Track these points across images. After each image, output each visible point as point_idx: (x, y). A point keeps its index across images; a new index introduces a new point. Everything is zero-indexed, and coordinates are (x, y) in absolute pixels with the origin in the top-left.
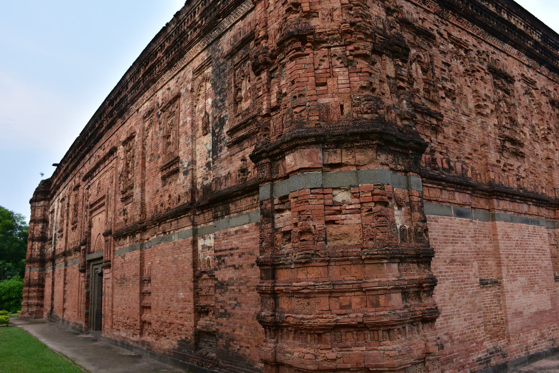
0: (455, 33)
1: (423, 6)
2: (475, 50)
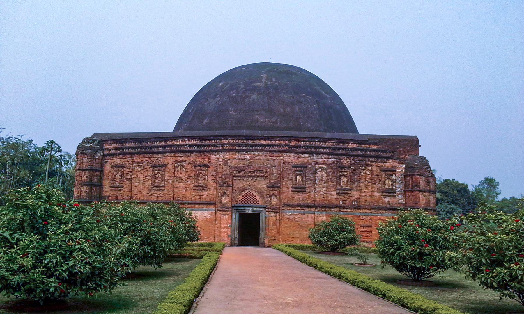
0: (136, 161)
1: (123, 158)
2: (146, 162)
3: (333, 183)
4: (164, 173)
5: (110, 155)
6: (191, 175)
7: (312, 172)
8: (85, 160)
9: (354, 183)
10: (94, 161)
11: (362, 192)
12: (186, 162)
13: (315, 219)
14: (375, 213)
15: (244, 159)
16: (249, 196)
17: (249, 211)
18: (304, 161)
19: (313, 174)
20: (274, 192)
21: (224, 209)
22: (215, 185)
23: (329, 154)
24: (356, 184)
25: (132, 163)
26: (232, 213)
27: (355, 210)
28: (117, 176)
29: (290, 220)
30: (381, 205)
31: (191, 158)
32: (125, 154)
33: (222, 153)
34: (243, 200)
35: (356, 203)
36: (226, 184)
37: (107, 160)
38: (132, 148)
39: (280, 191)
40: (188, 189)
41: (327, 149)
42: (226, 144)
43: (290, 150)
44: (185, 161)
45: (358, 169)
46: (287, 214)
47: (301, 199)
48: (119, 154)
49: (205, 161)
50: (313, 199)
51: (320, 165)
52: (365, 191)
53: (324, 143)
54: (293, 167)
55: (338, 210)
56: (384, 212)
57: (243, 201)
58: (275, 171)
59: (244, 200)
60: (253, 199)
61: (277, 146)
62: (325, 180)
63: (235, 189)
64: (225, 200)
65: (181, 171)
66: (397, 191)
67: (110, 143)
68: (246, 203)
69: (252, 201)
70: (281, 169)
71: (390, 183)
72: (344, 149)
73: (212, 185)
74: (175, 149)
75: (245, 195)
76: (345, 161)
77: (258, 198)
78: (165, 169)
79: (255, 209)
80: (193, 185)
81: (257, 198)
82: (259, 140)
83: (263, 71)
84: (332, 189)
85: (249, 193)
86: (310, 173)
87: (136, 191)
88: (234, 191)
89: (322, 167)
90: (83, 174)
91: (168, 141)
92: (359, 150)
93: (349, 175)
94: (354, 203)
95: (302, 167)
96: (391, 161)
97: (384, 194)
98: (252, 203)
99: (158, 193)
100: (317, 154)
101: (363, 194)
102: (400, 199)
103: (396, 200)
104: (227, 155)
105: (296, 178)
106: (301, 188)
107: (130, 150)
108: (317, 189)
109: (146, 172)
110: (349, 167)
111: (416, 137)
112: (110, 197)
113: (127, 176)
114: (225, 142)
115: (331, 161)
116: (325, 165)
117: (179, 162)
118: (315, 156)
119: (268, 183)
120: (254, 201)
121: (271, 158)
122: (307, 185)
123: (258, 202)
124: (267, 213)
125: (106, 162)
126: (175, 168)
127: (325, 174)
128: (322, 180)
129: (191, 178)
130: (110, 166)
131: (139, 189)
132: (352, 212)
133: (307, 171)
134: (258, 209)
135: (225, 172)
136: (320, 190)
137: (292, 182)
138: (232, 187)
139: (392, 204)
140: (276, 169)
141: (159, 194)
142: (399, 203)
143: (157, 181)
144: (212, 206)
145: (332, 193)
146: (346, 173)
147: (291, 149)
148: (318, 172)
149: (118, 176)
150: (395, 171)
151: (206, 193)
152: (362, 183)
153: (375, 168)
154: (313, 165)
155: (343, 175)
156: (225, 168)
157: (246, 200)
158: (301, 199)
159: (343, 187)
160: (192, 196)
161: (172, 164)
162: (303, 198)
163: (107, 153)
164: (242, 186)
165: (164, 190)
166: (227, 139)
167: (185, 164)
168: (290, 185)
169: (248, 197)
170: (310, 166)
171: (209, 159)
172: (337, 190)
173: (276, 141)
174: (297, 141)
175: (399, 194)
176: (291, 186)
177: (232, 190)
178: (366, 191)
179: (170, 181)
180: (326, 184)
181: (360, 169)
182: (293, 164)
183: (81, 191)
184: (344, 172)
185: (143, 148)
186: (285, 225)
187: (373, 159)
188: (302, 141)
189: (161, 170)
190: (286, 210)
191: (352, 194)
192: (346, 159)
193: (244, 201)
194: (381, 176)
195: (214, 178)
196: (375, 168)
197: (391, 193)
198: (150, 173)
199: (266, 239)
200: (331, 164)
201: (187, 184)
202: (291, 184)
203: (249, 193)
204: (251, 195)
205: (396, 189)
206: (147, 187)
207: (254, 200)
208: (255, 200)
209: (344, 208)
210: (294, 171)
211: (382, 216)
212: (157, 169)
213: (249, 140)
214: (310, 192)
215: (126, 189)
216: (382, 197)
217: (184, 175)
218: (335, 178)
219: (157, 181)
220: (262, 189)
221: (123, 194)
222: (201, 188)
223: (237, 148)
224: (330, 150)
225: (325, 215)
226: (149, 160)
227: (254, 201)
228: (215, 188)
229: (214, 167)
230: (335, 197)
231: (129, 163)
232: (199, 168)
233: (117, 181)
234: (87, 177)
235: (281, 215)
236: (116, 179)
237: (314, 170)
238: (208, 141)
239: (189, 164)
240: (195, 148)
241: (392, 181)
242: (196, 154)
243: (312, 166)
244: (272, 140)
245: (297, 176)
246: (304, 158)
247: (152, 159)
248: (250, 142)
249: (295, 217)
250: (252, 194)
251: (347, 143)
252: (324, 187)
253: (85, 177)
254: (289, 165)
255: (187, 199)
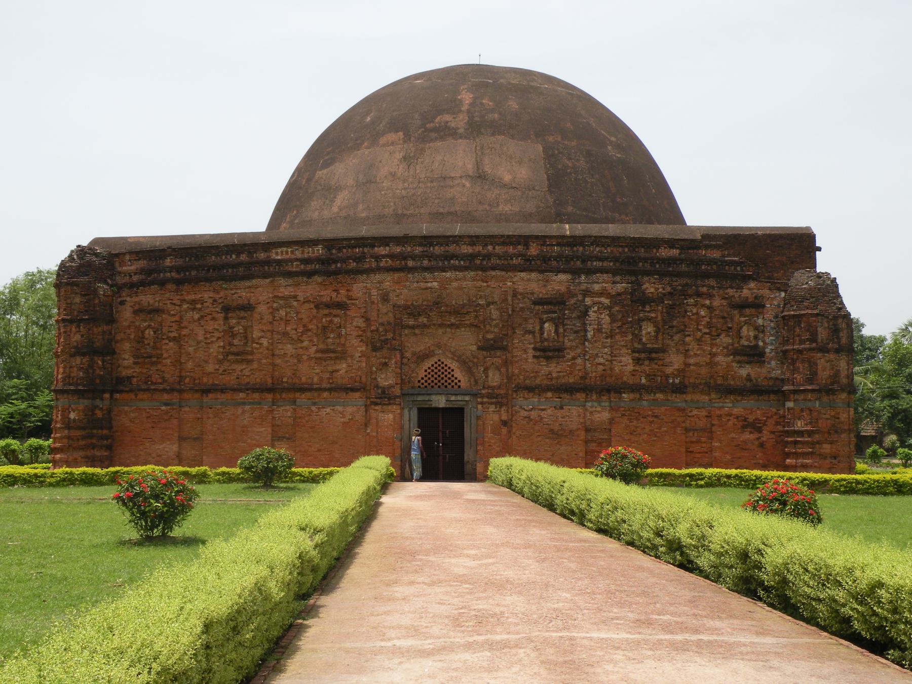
0: (191, 297)
2: (211, 301)
3: (625, 338)
4: (249, 324)
5: (131, 286)
6: (310, 327)
7: (579, 314)
8: (78, 300)
9: (672, 336)
10: (97, 302)
11: (690, 357)
12: (299, 298)
13: (584, 417)
14: (718, 401)
15: (427, 288)
16: (439, 371)
17: (440, 401)
18: (560, 290)
19: (579, 317)
20: (495, 359)
21: (384, 397)
22: (364, 348)
23: (615, 273)
24: (676, 338)
25: (178, 303)
26: (402, 409)
27: (674, 395)
28: (147, 332)
29: (531, 420)
30: (732, 383)
31: (311, 289)
32: (162, 283)
33: (377, 276)
34: (425, 379)
35: (677, 381)
36: (389, 346)
37: (124, 299)
38: (178, 269)
39: (506, 358)
40: (305, 357)
41: (610, 261)
42: (384, 256)
43: (528, 265)
44: (295, 297)
45: (680, 305)
46: (524, 409)
47: (554, 375)
48: (151, 283)
49: (339, 296)
50: (580, 374)
51: (595, 297)
52: (695, 354)
53: (603, 249)
54: (535, 303)
55: (638, 396)
56: (739, 398)
57: (426, 381)
58: (495, 314)
59: (429, 379)
60: (449, 376)
61: (500, 257)
62: (608, 331)
63: (408, 355)
64: (387, 379)
65: (288, 319)
66: (767, 350)
67: (130, 260)
68: (432, 387)
69: (446, 381)
70: (507, 309)
71: (752, 334)
72: (649, 261)
73: (357, 348)
74: (271, 269)
75: (429, 368)
76: (652, 287)
77: (459, 374)
78: (251, 315)
79: (453, 398)
80: (315, 348)
81: (458, 374)
82: (458, 245)
83: (466, 86)
84: (624, 351)
85: (440, 363)
86: (574, 315)
87: (190, 365)
88: (406, 360)
89: (600, 303)
90: (74, 329)
91: (255, 252)
92: (681, 261)
93: (659, 318)
94: (671, 381)
95: (555, 304)
96: (752, 285)
97: (738, 358)
98: (446, 387)
99: (239, 367)
100: (590, 272)
101: (692, 361)
102: (774, 370)
103: (764, 371)
104: (388, 281)
105: (542, 328)
106: (555, 350)
107: (173, 274)
108: (591, 352)
109: (212, 322)
110: (660, 299)
111: (808, 228)
112: (135, 379)
113: (169, 332)
114: (383, 251)
115: (620, 287)
116: (607, 298)
117: (282, 298)
118: (583, 277)
119: (480, 341)
120: (449, 381)
121: (485, 284)
122: (568, 344)
123: (458, 384)
124: (480, 406)
125: (123, 303)
126: (274, 311)
127: (607, 317)
128: (599, 330)
129: (310, 333)
130: (132, 310)
131: (197, 360)
132: (668, 400)
133: (566, 312)
134: (459, 398)
135: (384, 319)
136: (597, 354)
137: (534, 337)
138: (400, 350)
139: (757, 380)
140: (497, 309)
141: (241, 371)
142: (771, 378)
143: (236, 342)
144: (357, 395)
145: (623, 359)
146: (653, 315)
147: (530, 263)
148: (591, 313)
149: (149, 333)
150: (764, 306)
151: (344, 366)
152: (689, 335)
153: (717, 302)
154: (580, 297)
155: (649, 319)
156: (384, 309)
157: (433, 379)
158: (554, 375)
159: (648, 346)
160: (310, 372)
161: (268, 303)
162: (560, 372)
163: (124, 281)
164: (422, 348)
165: (252, 361)
166: (388, 245)
167: (295, 303)
168: (530, 344)
169: (436, 373)
170: (573, 301)
171: (348, 290)
172: (633, 352)
173: (497, 247)
174: (542, 245)
175: (771, 359)
176: (532, 346)
177: (402, 358)
178: (698, 352)
179: (265, 342)
180: (609, 340)
181: (684, 304)
182: (536, 296)
183: (71, 367)
184: (649, 312)
185: (204, 270)
186: (518, 433)
187: (712, 282)
188: (554, 245)
189: (243, 318)
190: (522, 399)
191: (667, 360)
192: (654, 283)
193: (429, 381)
194: (732, 319)
195: (361, 333)
196: (717, 302)
197: (754, 355)
198: (219, 324)
199: (478, 465)
200: (619, 294)
201: (301, 348)
202: (532, 341)
203: (440, 363)
204: (443, 368)
205: (764, 348)
206: (215, 354)
207: (449, 378)
208: (453, 379)
209: (648, 389)
210: (537, 314)
211: (733, 407)
212: (234, 315)
213: (436, 245)
214: (574, 358)
215: (169, 361)
216: (734, 365)
217: (295, 327)
218: (630, 325)
219: (236, 342)
220: (468, 354)
221: (164, 372)
222: (332, 355)
223: (411, 263)
224: (618, 264)
225: (608, 408)
226: (217, 296)
227: (449, 381)
228: (363, 355)
229: (360, 308)
230: (630, 368)
231: (174, 304)
232: (326, 311)
233: (149, 344)
234: (82, 336)
235: (510, 411)
236: (147, 339)
237: (582, 308)
238: (345, 251)
239: (304, 302)
240: (317, 266)
241: (756, 328)
242: (319, 279)
243: (578, 300)
244: (486, 245)
245: (544, 323)
246: (560, 282)
247: (222, 294)
248: (438, 250)
249: (542, 414)
250: (446, 365)
251: (654, 247)
252: (605, 347)
253: (78, 337)
254: (526, 300)
255: (304, 379)
